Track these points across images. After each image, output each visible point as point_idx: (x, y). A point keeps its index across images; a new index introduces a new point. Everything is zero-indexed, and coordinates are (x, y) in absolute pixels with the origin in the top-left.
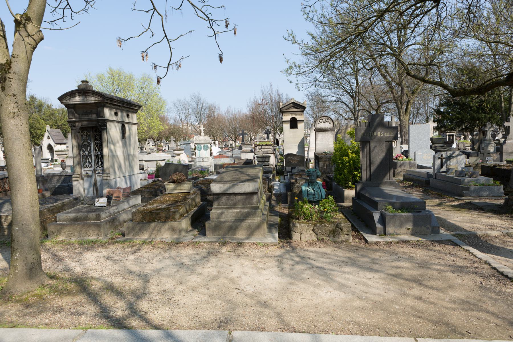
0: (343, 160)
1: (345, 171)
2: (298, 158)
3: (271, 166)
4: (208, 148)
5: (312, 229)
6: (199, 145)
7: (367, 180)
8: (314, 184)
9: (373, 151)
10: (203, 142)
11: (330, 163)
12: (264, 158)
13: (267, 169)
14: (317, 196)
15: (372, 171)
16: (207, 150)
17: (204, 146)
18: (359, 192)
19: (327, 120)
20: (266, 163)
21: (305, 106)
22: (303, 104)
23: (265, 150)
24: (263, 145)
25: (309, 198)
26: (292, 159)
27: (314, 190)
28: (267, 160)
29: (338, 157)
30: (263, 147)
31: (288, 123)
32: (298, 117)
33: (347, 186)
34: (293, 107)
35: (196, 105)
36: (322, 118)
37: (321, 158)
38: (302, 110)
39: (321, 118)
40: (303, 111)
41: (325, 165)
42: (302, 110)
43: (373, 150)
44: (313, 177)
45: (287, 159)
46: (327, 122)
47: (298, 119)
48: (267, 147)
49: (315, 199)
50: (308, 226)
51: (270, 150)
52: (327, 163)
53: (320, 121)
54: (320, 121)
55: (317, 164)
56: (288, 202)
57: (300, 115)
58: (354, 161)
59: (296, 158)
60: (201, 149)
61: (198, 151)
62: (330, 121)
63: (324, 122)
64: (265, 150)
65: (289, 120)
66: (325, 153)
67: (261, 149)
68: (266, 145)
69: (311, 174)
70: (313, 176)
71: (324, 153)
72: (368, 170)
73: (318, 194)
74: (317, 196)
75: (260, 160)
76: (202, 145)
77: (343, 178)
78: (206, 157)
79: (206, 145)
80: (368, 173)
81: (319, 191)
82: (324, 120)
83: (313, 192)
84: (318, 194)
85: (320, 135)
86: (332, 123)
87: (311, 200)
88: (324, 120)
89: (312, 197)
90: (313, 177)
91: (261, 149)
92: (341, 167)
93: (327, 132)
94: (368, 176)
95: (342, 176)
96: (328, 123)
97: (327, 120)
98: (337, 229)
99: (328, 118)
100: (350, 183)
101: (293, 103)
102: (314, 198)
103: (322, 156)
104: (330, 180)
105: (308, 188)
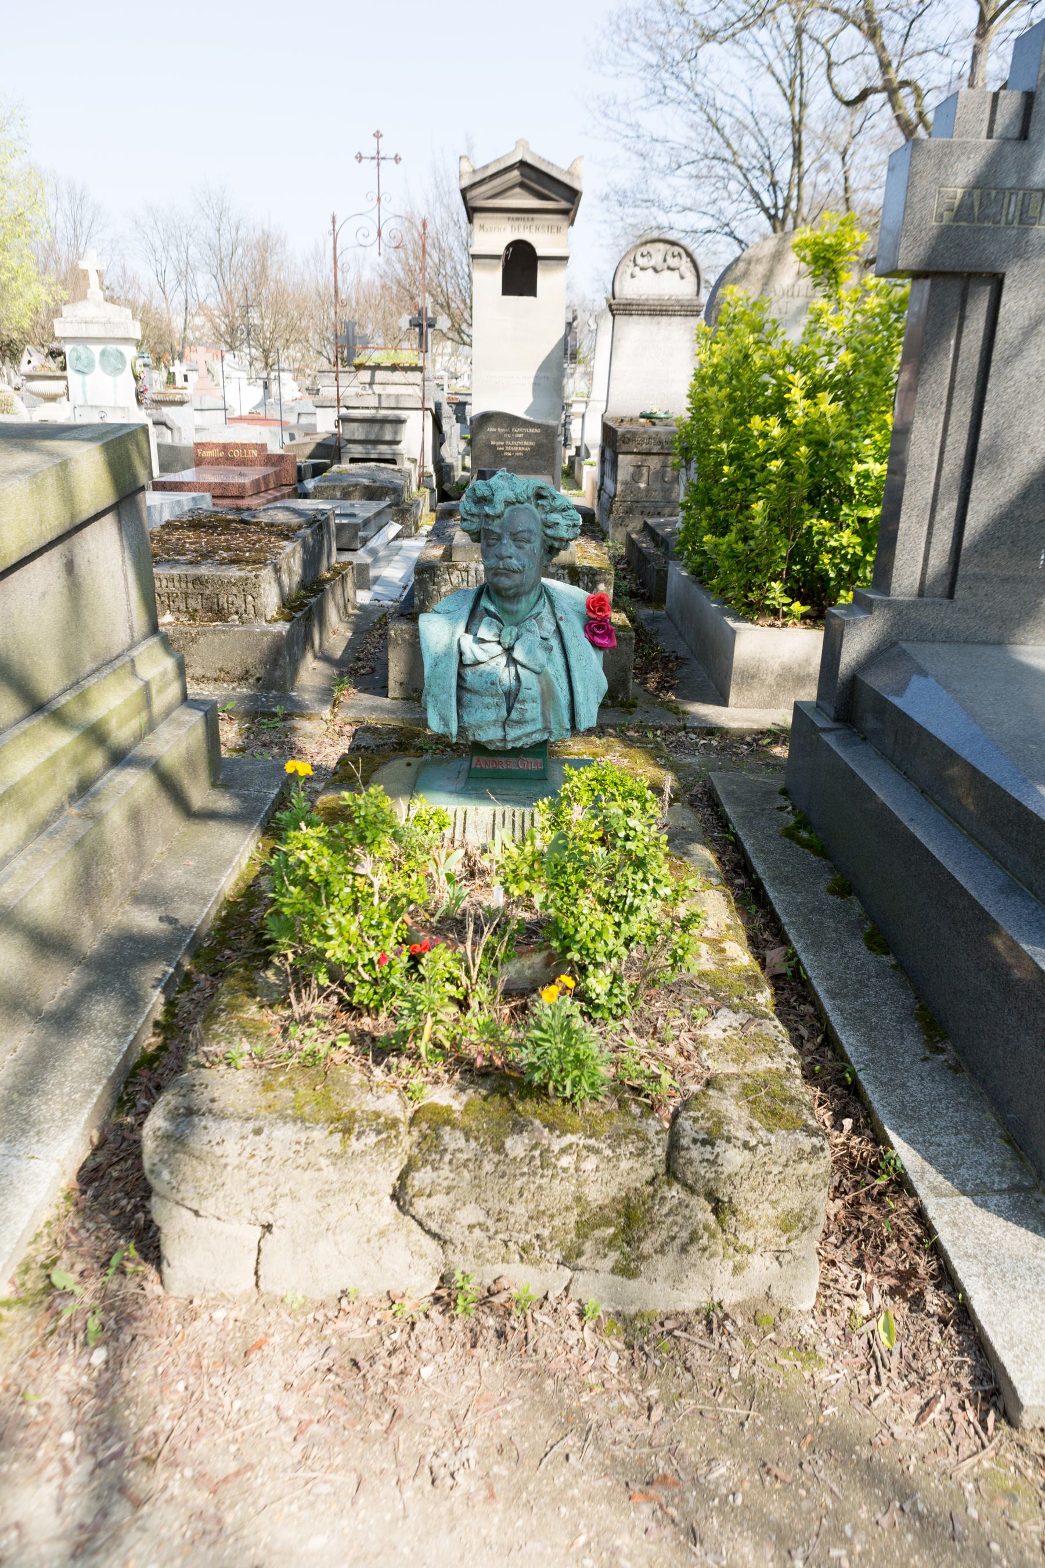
0: (746, 440)
1: (758, 507)
2: (528, 437)
3: (407, 465)
4: (123, 361)
5: (387, 1181)
6: (80, 348)
7: (921, 593)
8: (522, 606)
9: (1008, 361)
10: (95, 331)
11: (664, 466)
12: (377, 427)
13: (383, 476)
14: (533, 710)
15: (976, 520)
16: (117, 371)
17: (103, 353)
18: (853, 680)
19: (672, 262)
20: (383, 448)
21: (576, 185)
22: (569, 173)
23: (391, 390)
24: (378, 367)
25: (469, 719)
26: (501, 438)
27: (512, 661)
28: (388, 437)
29: (718, 418)
30: (380, 375)
31: (495, 267)
32: (543, 243)
33: (750, 605)
34: (522, 185)
35: (212, 233)
36: (649, 248)
37: (629, 438)
38: (563, 205)
39: (644, 249)
40: (568, 214)
41: (645, 470)
42: (563, 205)
43: (1018, 351)
44: (509, 547)
45: (482, 437)
46: (669, 268)
47: (540, 252)
48: (398, 376)
49: (513, 733)
50: (336, 1158)
51: (410, 390)
52: (654, 463)
53: (640, 261)
54: (640, 261)
55: (608, 467)
56: (391, 684)
57: (550, 228)
58: (818, 444)
59: (519, 431)
60: (90, 365)
61: (80, 377)
62: (685, 264)
63: (656, 270)
64: (391, 390)
65: (500, 250)
66: (649, 417)
67: (371, 384)
68: (394, 368)
69: (495, 526)
70: (515, 537)
71: (642, 416)
72: (948, 509)
73: (547, 695)
74: (533, 710)
75: (358, 432)
76: (96, 349)
77: (733, 555)
78: (114, 408)
79: (111, 347)
80: (944, 538)
81: (555, 669)
82: (657, 259)
83: (506, 676)
84: (547, 695)
85: (635, 329)
86: (691, 277)
87: (483, 736)
88: (657, 259)
89: (491, 715)
90: (509, 547)
91: (371, 384)
92: (732, 483)
93: (664, 320)
94: (939, 559)
95: (731, 537)
96: (676, 274)
97: (672, 262)
98: (675, 1192)
99: (676, 250)
100: (777, 586)
101: (523, 164)
102: (504, 724)
103: (633, 427)
104: (657, 546)
105: (467, 641)
